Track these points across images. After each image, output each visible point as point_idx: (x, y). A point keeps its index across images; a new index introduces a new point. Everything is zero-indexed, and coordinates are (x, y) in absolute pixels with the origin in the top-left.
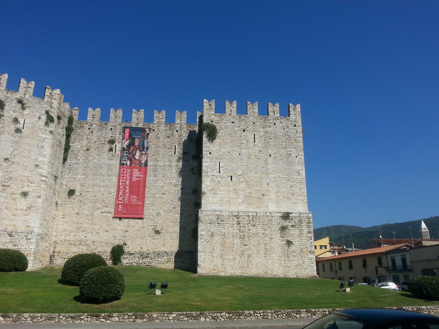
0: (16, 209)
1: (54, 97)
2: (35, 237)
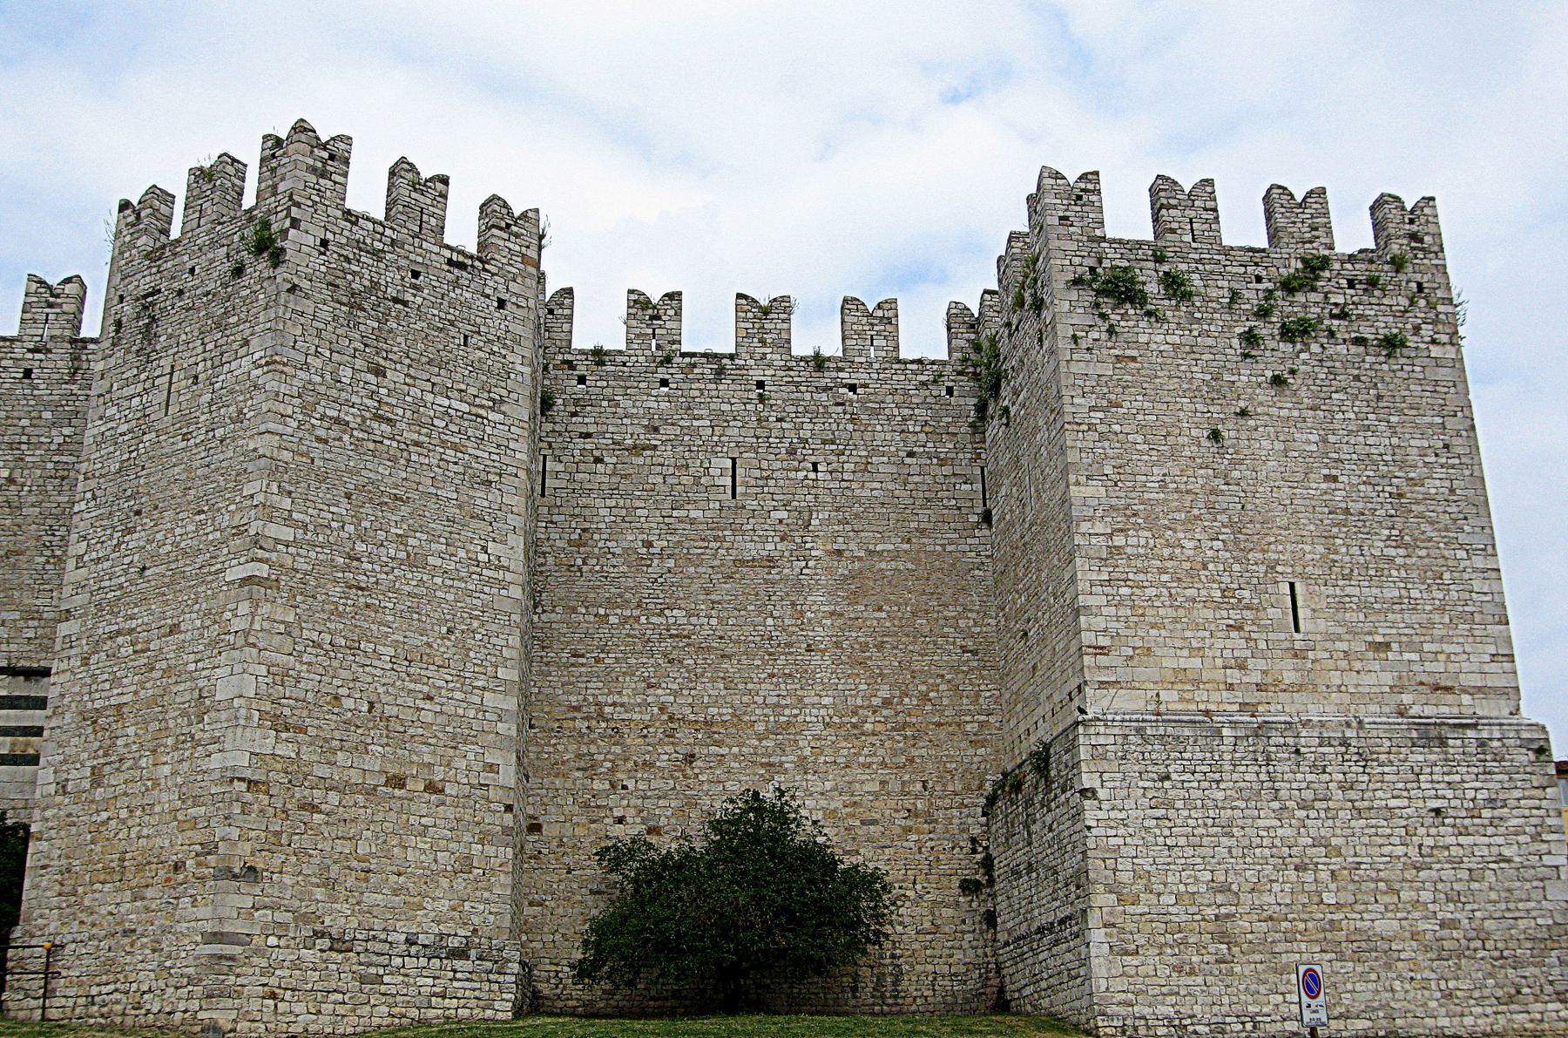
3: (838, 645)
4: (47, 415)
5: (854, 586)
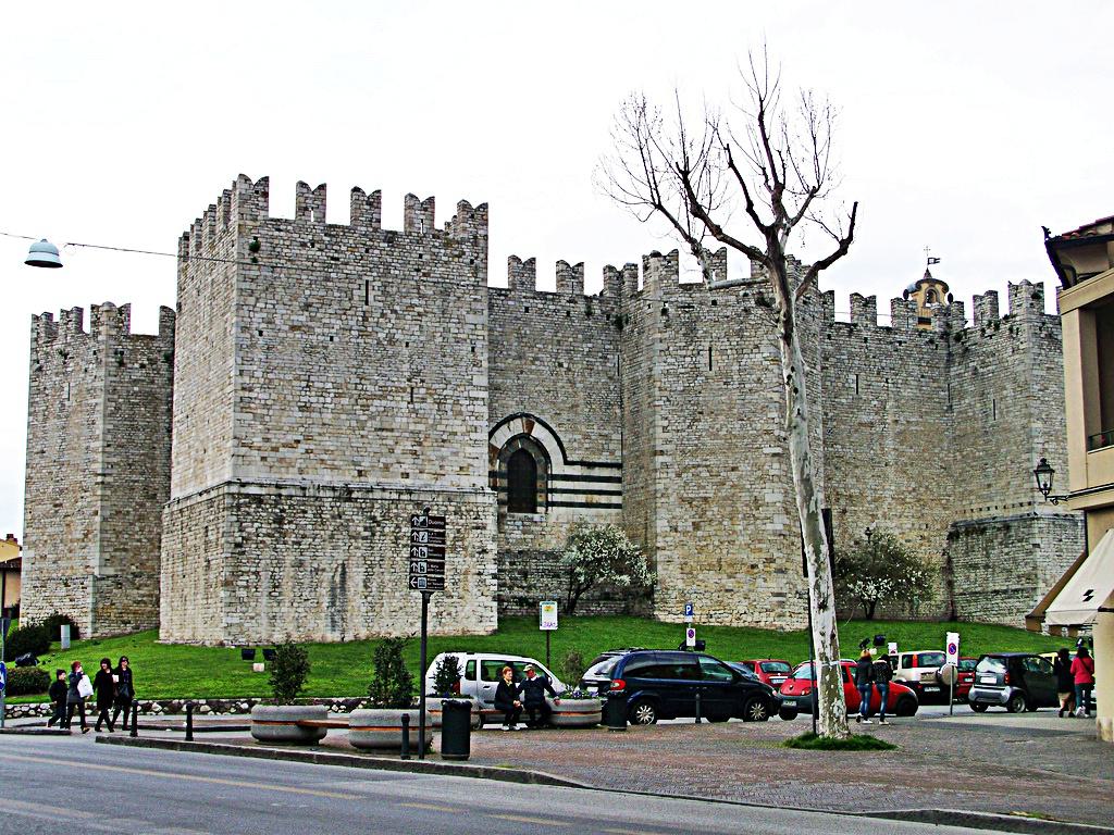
0: (71, 541)
2: (91, 584)
3: (896, 463)
4: (580, 336)
5: (901, 436)
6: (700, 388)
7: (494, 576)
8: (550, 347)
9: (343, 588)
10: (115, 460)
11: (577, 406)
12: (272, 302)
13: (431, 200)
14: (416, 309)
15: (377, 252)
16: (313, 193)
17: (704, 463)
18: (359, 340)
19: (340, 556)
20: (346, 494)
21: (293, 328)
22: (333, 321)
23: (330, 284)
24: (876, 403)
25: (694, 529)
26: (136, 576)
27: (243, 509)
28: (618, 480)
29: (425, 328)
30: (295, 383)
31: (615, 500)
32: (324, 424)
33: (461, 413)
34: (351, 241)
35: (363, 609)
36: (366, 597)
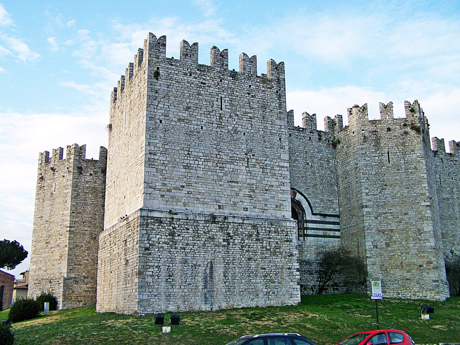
1: (71, 152)
2: (62, 282)
4: (316, 150)
6: (384, 172)
7: (298, 270)
8: (302, 154)
9: (211, 277)
10: (76, 220)
11: (317, 185)
12: (168, 104)
13: (254, 57)
14: (249, 115)
15: (226, 81)
16: (191, 47)
17: (389, 211)
18: (217, 130)
19: (209, 257)
20: (213, 219)
21: (180, 120)
22: (203, 118)
23: (201, 97)
24: (448, 189)
25: (386, 246)
26: (85, 278)
27: (150, 226)
28: (338, 224)
29: (254, 126)
30: (181, 152)
31: (337, 234)
32: (198, 177)
33: (275, 174)
34: (212, 75)
35: (224, 290)
36: (225, 283)
